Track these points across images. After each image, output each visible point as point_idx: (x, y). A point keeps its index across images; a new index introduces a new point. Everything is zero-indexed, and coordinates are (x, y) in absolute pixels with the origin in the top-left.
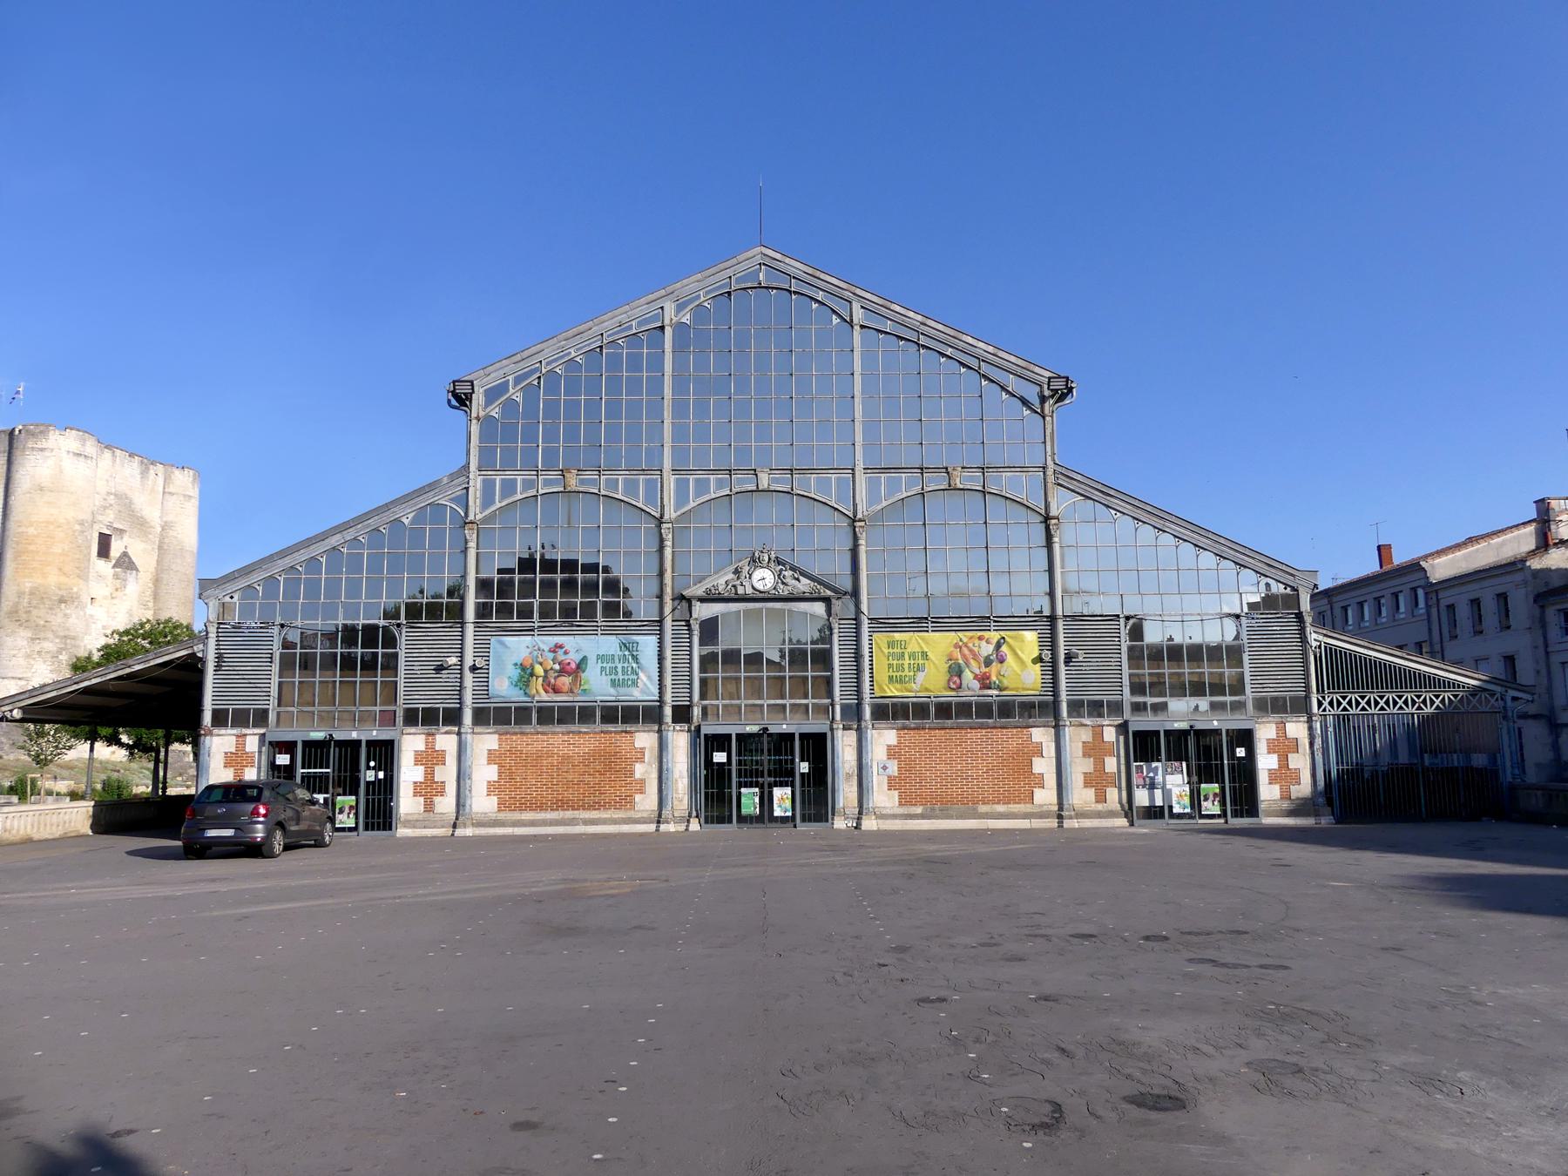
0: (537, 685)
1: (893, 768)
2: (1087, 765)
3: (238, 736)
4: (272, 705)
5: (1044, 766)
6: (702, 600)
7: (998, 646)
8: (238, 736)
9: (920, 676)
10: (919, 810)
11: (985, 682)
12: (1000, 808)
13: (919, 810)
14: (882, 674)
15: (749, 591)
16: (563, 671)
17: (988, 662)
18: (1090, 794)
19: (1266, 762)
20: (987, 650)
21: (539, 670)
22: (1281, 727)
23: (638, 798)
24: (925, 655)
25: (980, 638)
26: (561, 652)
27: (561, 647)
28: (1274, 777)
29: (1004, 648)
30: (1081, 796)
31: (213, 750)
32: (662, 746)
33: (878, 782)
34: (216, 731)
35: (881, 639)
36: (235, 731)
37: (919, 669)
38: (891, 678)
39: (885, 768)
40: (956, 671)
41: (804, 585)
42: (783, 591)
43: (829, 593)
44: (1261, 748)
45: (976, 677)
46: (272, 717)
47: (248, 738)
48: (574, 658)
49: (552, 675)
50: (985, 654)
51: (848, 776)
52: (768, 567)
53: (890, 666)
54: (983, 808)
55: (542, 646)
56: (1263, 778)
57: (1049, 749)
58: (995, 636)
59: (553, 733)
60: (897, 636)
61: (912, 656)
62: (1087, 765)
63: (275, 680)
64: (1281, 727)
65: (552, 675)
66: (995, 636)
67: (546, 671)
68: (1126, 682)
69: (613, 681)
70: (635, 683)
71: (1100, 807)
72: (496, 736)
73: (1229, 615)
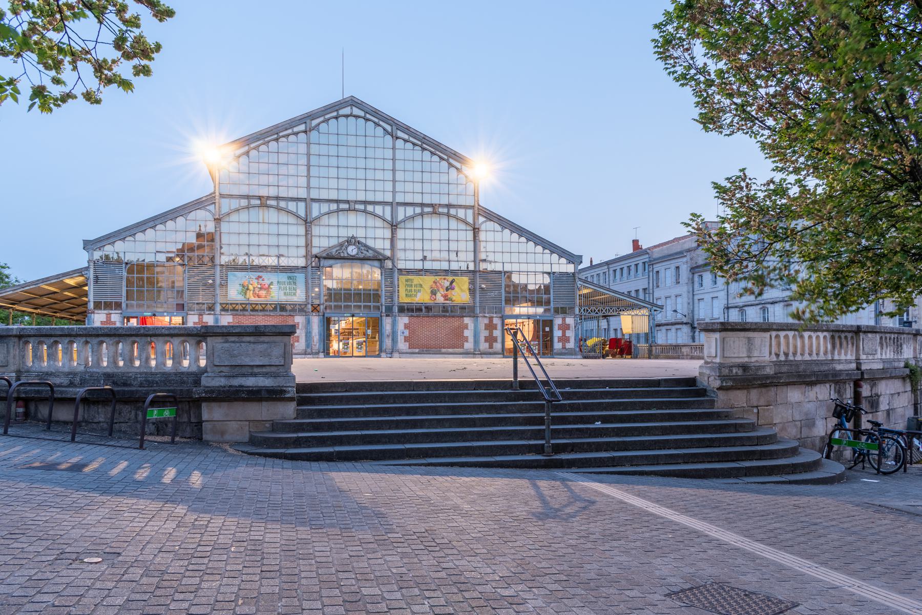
0: (250, 295)
1: (407, 333)
2: (486, 333)
3: (107, 314)
4: (124, 299)
5: (468, 333)
6: (325, 258)
7: (452, 282)
8: (107, 314)
9: (419, 294)
10: (417, 350)
11: (446, 297)
12: (451, 350)
13: (417, 350)
14: (402, 293)
15: (346, 255)
16: (261, 289)
17: (447, 289)
18: (487, 345)
19: (557, 333)
20: (447, 284)
21: (251, 287)
22: (564, 319)
23: (296, 344)
24: (421, 286)
25: (444, 279)
26: (260, 280)
27: (261, 277)
28: (560, 340)
29: (454, 284)
30: (484, 346)
31: (95, 320)
32: (308, 322)
33: (400, 339)
34: (96, 311)
35: (403, 278)
36: (105, 312)
37: (419, 291)
38: (406, 295)
39: (403, 333)
40: (434, 293)
41: (370, 254)
42: (361, 256)
43: (381, 257)
44: (556, 328)
45: (442, 296)
46: (124, 305)
47: (112, 315)
48: (267, 282)
49: (257, 290)
50: (446, 286)
51: (388, 336)
52: (354, 245)
53: (406, 290)
54: (443, 350)
55: (252, 277)
56: (556, 340)
57: (471, 326)
58: (450, 278)
59: (258, 315)
60: (409, 277)
61: (416, 286)
62: (486, 333)
63: (124, 289)
64: (564, 319)
65: (257, 290)
66: (450, 278)
67: (254, 288)
68: (503, 299)
69: (285, 293)
70: (295, 294)
71: (491, 350)
72: (231, 316)
73: (546, 273)
